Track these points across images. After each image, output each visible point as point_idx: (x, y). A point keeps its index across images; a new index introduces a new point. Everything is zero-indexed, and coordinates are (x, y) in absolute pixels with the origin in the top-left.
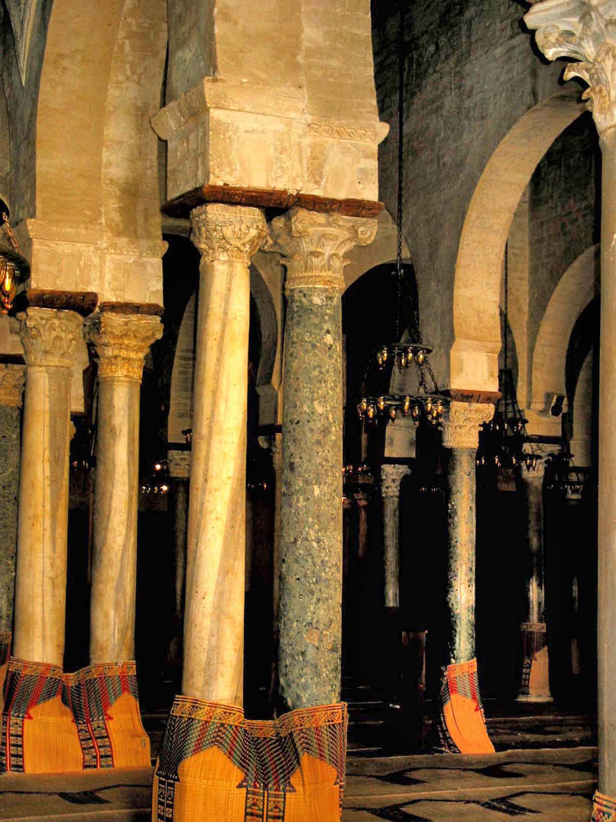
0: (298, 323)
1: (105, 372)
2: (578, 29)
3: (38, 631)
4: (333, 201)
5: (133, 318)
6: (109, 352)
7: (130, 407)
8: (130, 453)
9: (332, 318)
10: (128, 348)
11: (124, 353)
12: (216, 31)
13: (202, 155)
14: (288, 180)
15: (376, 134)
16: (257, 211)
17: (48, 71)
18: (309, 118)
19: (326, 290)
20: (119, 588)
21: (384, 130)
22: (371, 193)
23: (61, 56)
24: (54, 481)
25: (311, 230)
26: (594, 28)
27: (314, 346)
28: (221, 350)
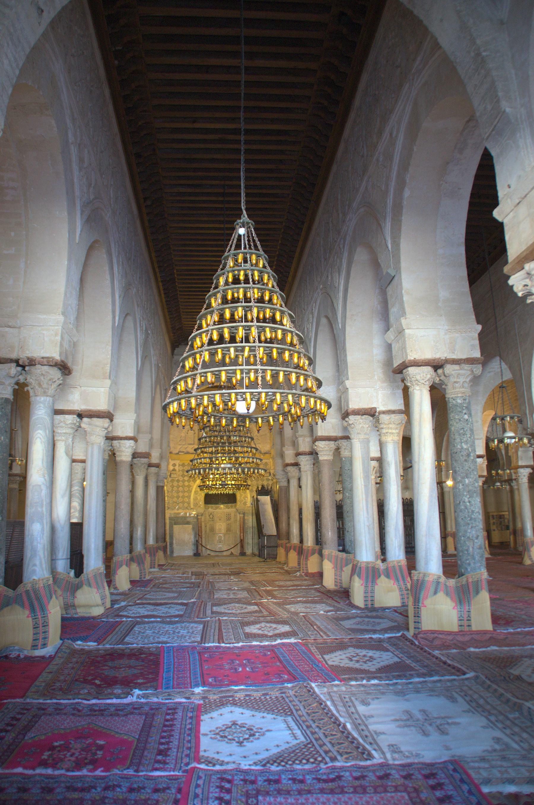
3: (364, 548)
4: (461, 360)
5: (393, 416)
6: (384, 431)
7: (395, 452)
8: (396, 472)
10: (391, 428)
11: (390, 431)
12: (404, 299)
13: (403, 348)
14: (441, 354)
15: (476, 330)
16: (429, 367)
17: (348, 322)
18: (446, 327)
20: (396, 529)
21: (479, 327)
22: (477, 354)
23: (353, 315)
25: (453, 372)
27: (460, 420)
28: (420, 426)
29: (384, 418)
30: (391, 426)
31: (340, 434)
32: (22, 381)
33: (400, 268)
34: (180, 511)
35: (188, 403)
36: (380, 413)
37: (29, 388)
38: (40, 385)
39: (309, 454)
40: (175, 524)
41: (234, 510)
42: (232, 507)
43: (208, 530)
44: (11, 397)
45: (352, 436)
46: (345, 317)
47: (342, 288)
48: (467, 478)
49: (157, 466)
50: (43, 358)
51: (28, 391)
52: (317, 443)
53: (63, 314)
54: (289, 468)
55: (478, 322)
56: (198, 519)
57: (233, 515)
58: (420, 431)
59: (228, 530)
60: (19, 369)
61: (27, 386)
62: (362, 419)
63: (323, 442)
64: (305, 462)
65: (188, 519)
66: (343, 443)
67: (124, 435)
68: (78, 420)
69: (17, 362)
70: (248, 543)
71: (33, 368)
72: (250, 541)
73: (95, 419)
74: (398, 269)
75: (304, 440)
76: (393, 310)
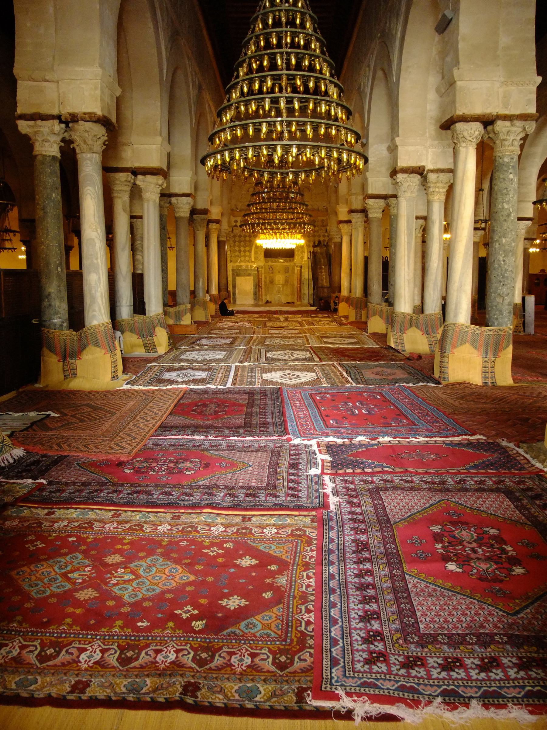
0: (498, 171)
4: (513, 116)
6: (431, 190)
7: (440, 211)
10: (438, 187)
11: (437, 190)
19: (510, 155)
21: (539, 79)
22: (532, 110)
25: (503, 130)
29: (432, 177)
30: (438, 185)
31: (390, 193)
32: (68, 138)
34: (242, 264)
35: (223, 159)
37: (75, 145)
38: (85, 142)
40: (238, 276)
41: (292, 263)
42: (290, 261)
43: (268, 282)
44: (59, 155)
49: (218, 222)
50: (84, 113)
51: (74, 148)
53: (101, 66)
54: (341, 226)
56: (258, 271)
57: (291, 268)
59: (287, 281)
60: (63, 126)
61: (73, 143)
62: (408, 177)
65: (249, 272)
66: (392, 201)
67: (181, 192)
68: (133, 177)
69: (59, 117)
70: (304, 294)
71: (76, 125)
72: (306, 292)
73: (149, 177)
74: (456, 10)
75: (356, 198)
76: (448, 59)
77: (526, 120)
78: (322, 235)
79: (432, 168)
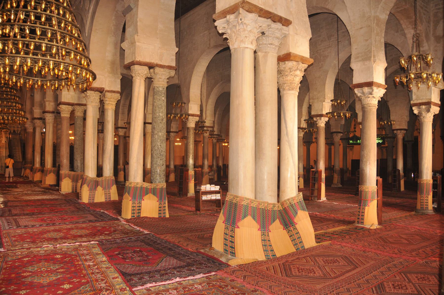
1: (106, 107)
2: (226, 27)
3: (90, 169)
4: (165, 66)
5: (113, 94)
6: (107, 102)
7: (112, 116)
8: (112, 127)
9: (164, 93)
10: (112, 101)
11: (111, 103)
13: (134, 53)
14: (154, 60)
16: (147, 67)
21: (177, 49)
22: (174, 64)
24: (94, 133)
25: (159, 72)
26: (230, 27)
29: (108, 95)
31: (76, 102)
33: (138, 5)
36: (106, 91)
39: (52, 113)
45: (88, 103)
46: (91, 30)
47: (91, 11)
48: (161, 132)
52: (61, 106)
54: (36, 121)
55: (177, 47)
58: (138, 103)
63: (65, 106)
64: (49, 118)
66: (78, 108)
74: (137, 5)
75: (49, 104)
77: (170, 69)
78: (16, 126)
79: (108, 89)
